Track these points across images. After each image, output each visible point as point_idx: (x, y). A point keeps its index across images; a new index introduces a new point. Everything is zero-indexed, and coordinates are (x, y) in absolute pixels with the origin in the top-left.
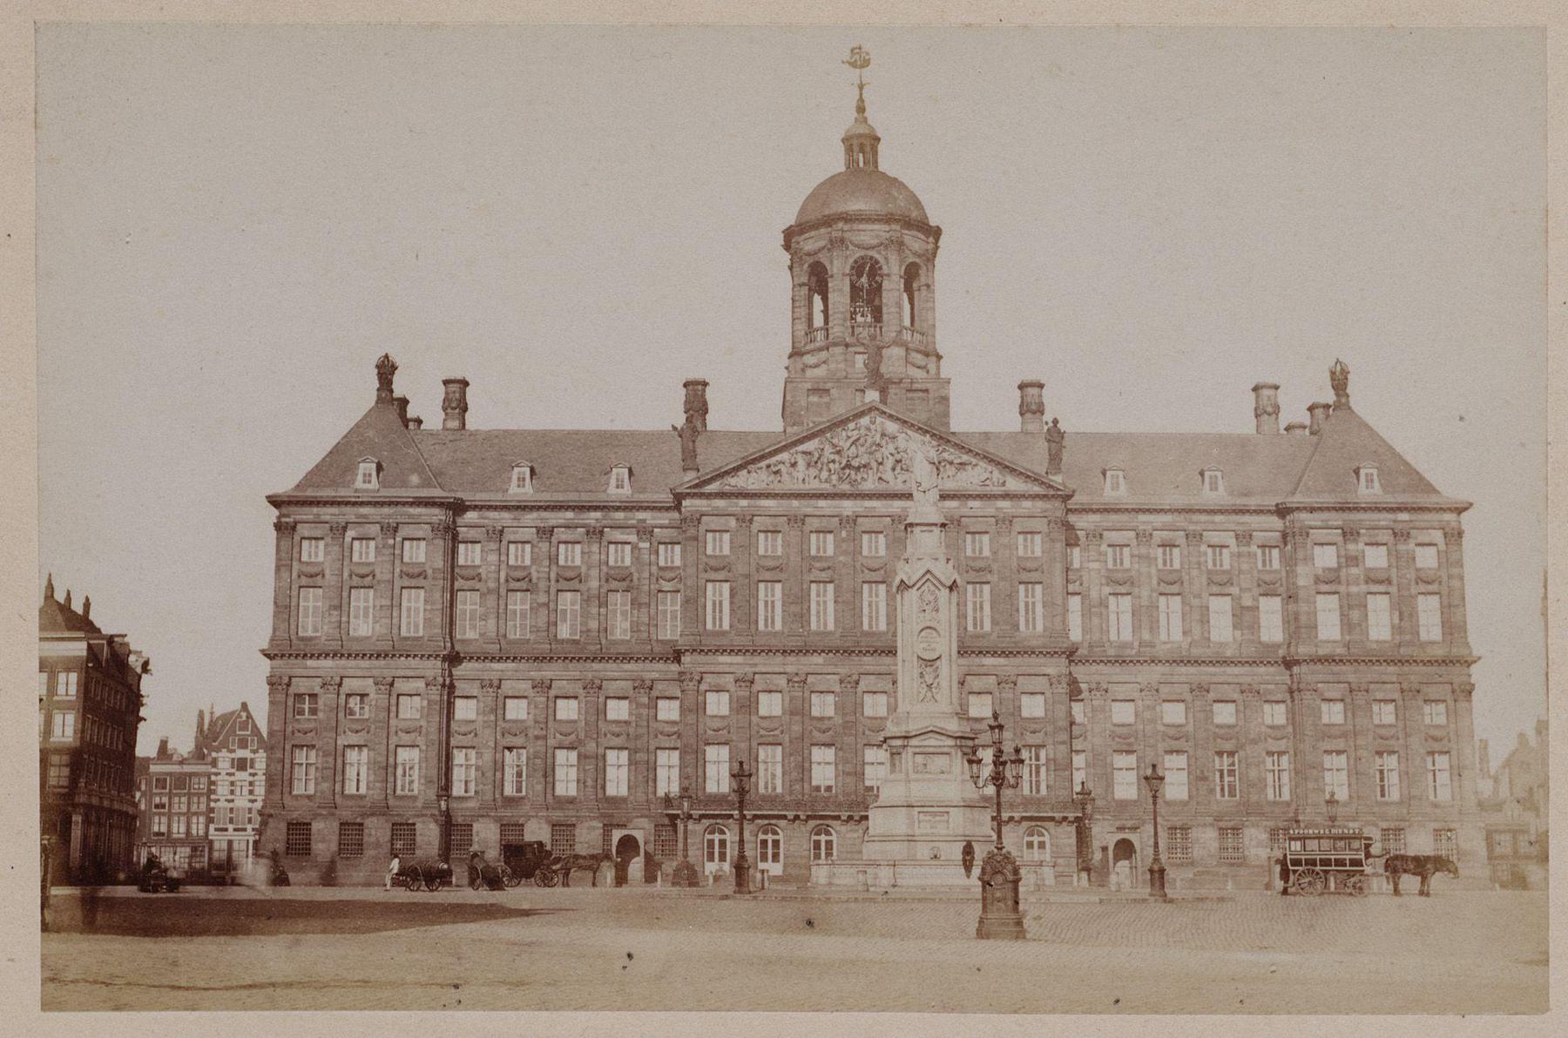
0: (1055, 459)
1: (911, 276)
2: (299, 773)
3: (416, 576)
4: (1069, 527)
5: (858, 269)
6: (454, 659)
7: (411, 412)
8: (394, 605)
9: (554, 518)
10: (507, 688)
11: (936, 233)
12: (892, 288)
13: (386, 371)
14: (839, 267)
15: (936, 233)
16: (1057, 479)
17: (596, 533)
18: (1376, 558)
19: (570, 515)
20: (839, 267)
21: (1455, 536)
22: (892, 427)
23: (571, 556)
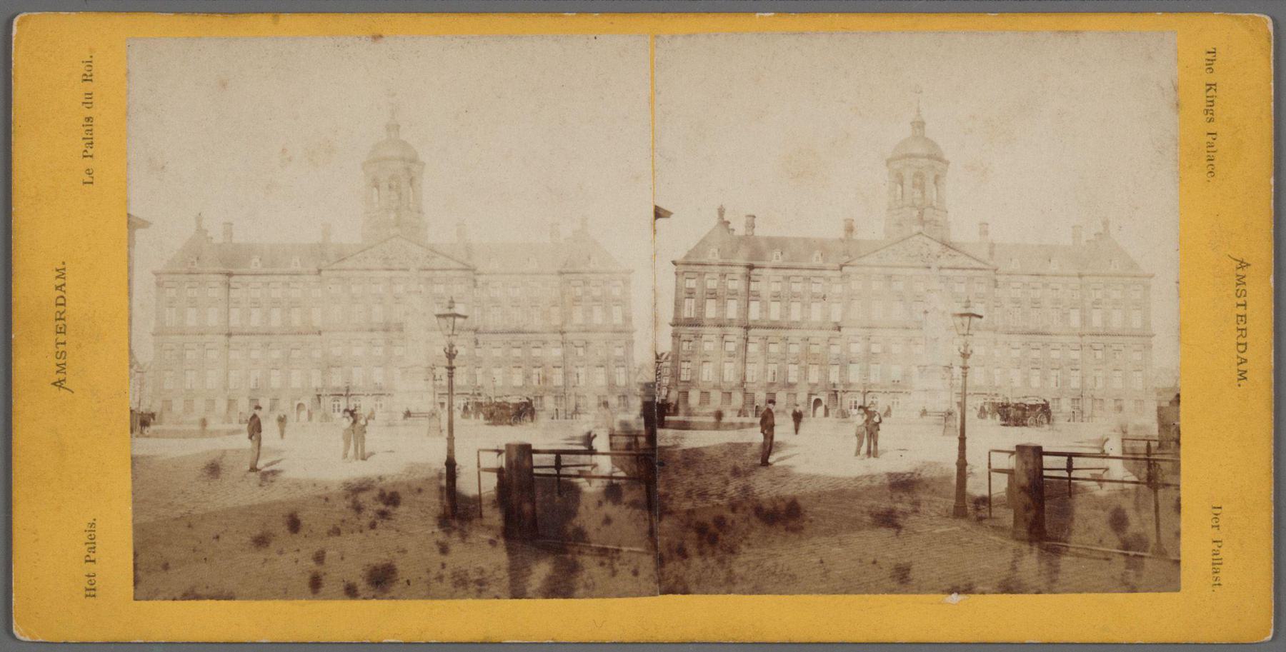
0: (991, 254)
1: (937, 178)
2: (684, 372)
3: (734, 294)
4: (996, 281)
5: (916, 175)
6: (747, 328)
7: (731, 226)
8: (724, 305)
9: (789, 272)
10: (770, 340)
11: (948, 163)
12: (929, 183)
13: (721, 212)
14: (908, 174)
15: (948, 163)
16: (992, 263)
17: (807, 279)
18: (1116, 295)
19: (796, 272)
20: (908, 174)
21: (1147, 287)
22: (927, 240)
23: (797, 288)
